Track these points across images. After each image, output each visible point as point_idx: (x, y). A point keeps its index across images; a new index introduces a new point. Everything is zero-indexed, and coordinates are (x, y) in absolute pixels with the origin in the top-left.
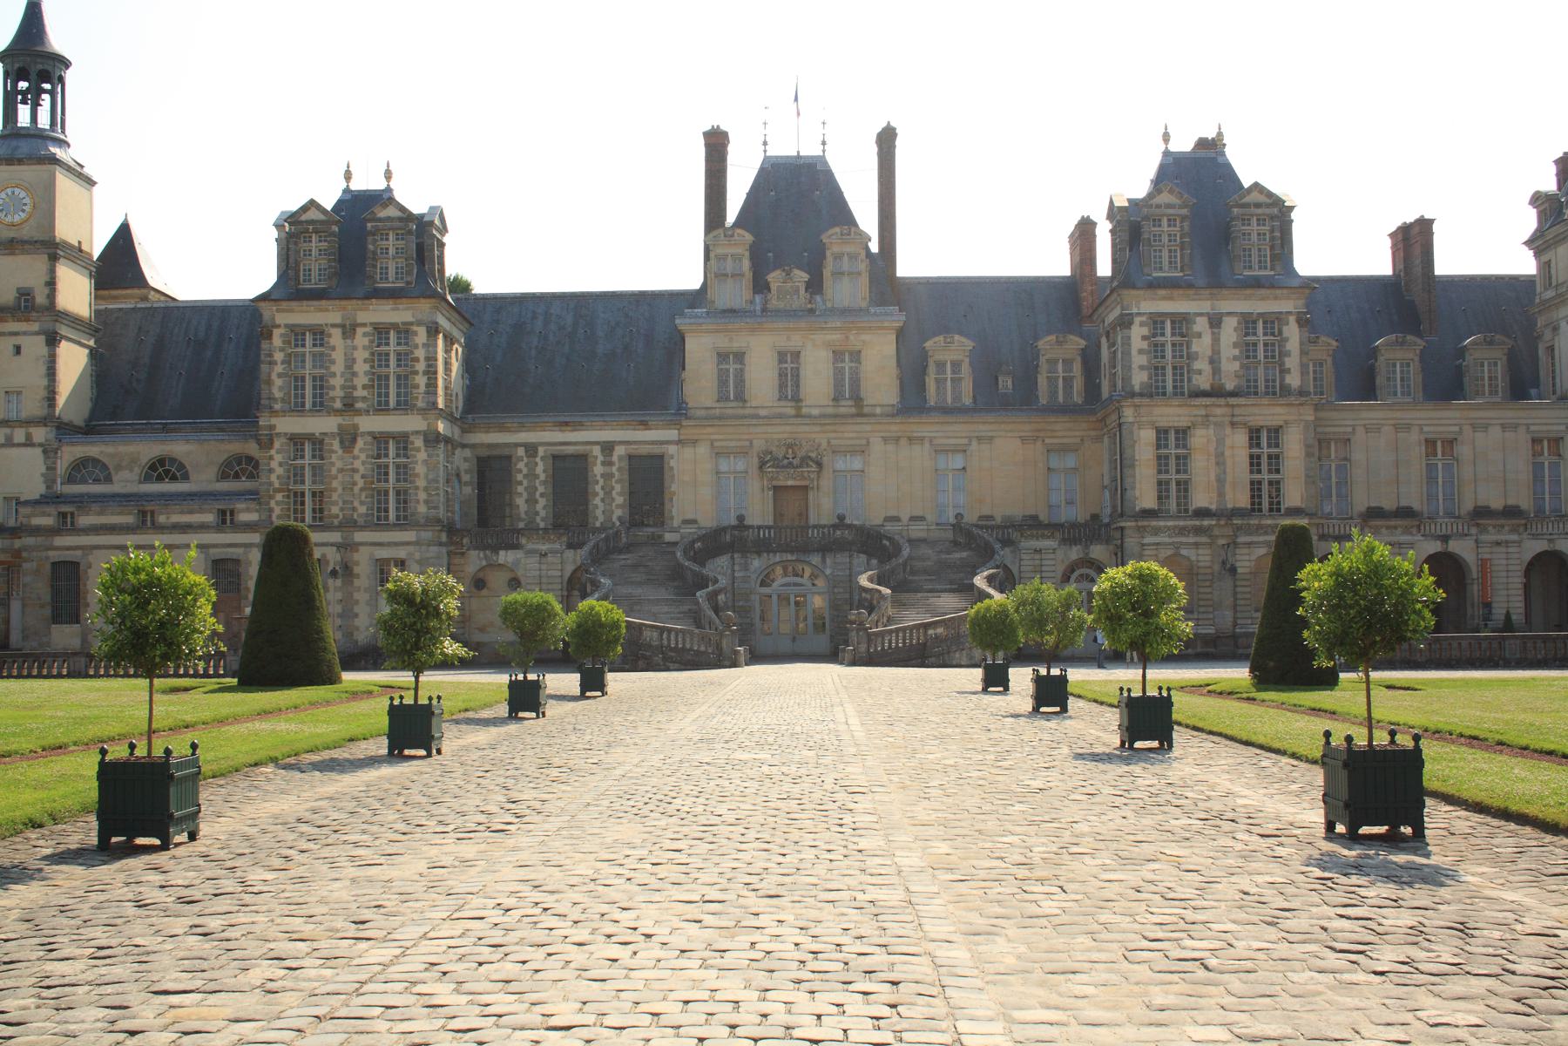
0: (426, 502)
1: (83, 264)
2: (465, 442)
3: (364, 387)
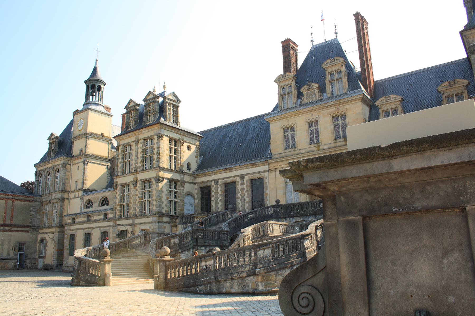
0: (156, 205)
1: (104, 140)
2: (195, 182)
3: (140, 163)
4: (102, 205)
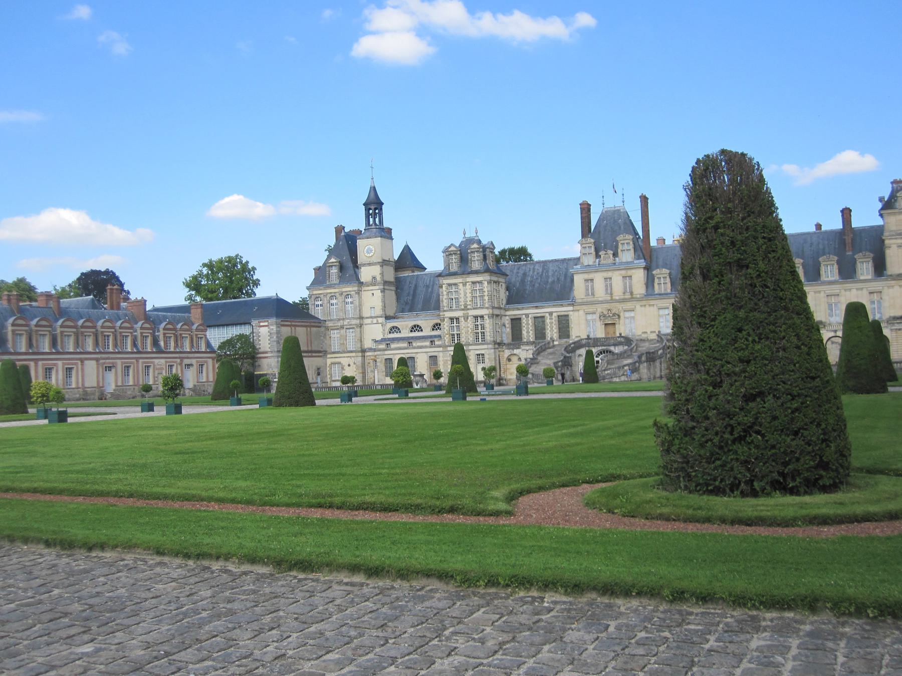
4: (411, 331)
